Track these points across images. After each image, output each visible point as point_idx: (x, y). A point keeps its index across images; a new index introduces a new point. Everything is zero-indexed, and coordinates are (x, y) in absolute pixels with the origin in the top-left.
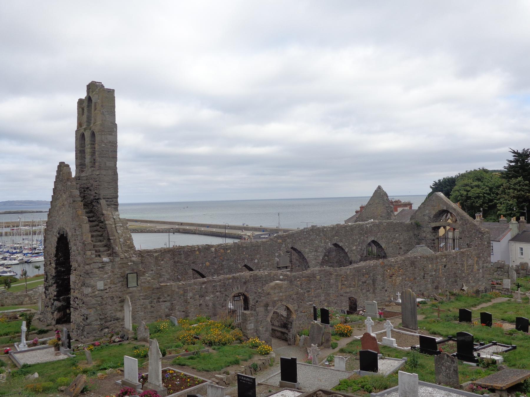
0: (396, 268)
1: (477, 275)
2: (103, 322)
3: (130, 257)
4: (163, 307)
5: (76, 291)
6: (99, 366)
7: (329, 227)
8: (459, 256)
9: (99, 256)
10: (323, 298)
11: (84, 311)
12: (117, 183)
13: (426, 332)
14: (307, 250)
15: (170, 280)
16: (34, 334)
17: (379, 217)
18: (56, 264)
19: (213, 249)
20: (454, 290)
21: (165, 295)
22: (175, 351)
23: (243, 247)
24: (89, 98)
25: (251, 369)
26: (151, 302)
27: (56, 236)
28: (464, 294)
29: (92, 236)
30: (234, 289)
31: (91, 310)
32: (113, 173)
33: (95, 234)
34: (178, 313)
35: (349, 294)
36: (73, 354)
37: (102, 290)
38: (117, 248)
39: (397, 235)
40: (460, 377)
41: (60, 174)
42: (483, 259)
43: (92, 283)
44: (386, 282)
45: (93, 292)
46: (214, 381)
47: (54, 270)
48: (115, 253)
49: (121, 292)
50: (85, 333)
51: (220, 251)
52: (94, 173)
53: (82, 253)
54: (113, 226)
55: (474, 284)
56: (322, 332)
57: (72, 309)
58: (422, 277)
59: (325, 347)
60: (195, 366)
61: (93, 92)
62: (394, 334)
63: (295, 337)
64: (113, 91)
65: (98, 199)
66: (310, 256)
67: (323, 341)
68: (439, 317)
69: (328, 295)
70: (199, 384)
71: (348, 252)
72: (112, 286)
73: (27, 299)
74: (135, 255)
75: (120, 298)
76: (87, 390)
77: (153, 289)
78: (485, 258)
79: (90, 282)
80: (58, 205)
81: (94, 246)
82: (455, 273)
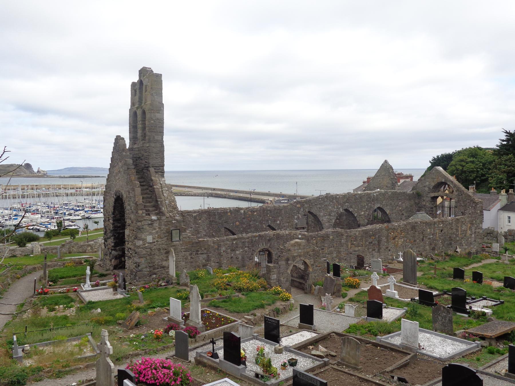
0: (399, 231)
1: (470, 239)
2: (151, 269)
3: (174, 217)
4: (201, 258)
5: (130, 243)
6: (149, 305)
7: (341, 195)
8: (454, 222)
9: (149, 215)
10: (335, 255)
11: (136, 260)
12: (163, 154)
13: (424, 287)
14: (322, 214)
15: (206, 236)
16: (96, 277)
17: (385, 187)
18: (113, 221)
19: (242, 211)
20: (449, 251)
21: (203, 249)
22: (211, 295)
23: (267, 210)
24: (141, 82)
25: (274, 312)
26: (191, 254)
27: (113, 197)
28: (457, 255)
29: (143, 198)
30: (259, 245)
31: (142, 259)
32: (160, 146)
33: (145, 196)
34: (213, 264)
35: (357, 253)
36: (128, 294)
37: (151, 243)
38: (163, 209)
39: (400, 203)
40: (454, 326)
41: (117, 145)
42: (476, 226)
43: (143, 237)
44: (389, 243)
45: (144, 245)
46: (244, 321)
47: (111, 225)
48: (162, 212)
49: (167, 245)
50: (137, 278)
51: (248, 213)
52: (145, 145)
53: (135, 212)
54: (160, 190)
55: (466, 247)
56: (334, 284)
57: (126, 258)
58: (421, 240)
59: (336, 296)
60: (227, 308)
61: (144, 76)
62: (396, 288)
63: (311, 287)
64: (161, 75)
65: (148, 167)
66: (324, 219)
67: (335, 291)
68: (435, 274)
69: (339, 252)
70: (231, 323)
71: (357, 216)
72: (159, 240)
73: (89, 248)
74: (178, 214)
75: (166, 250)
76: (140, 324)
77: (193, 244)
78: (478, 224)
79: (141, 236)
80: (115, 172)
81: (145, 206)
82: (450, 237)
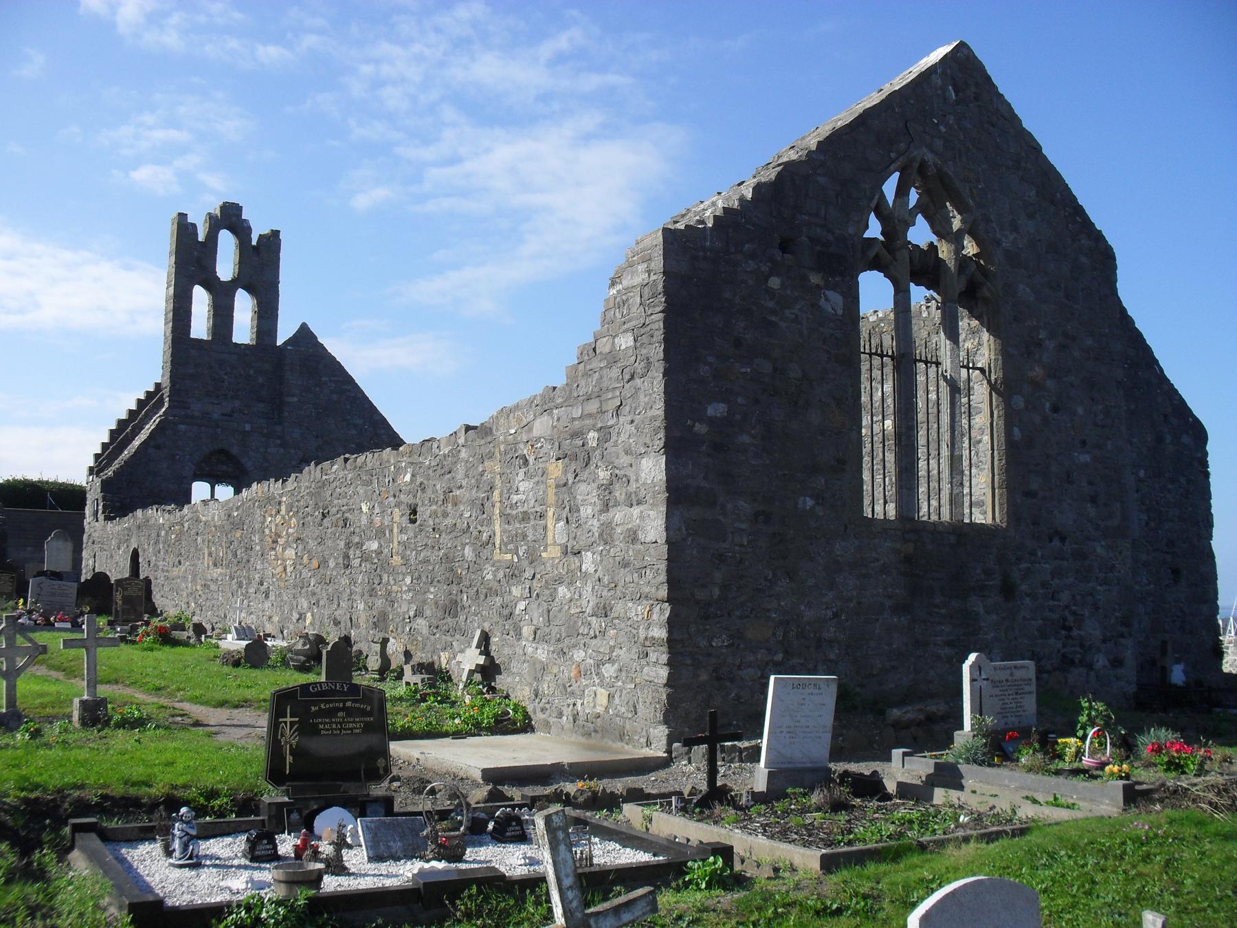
1: (562, 591)
8: (464, 454)
42: (603, 475)
58: (341, 560)
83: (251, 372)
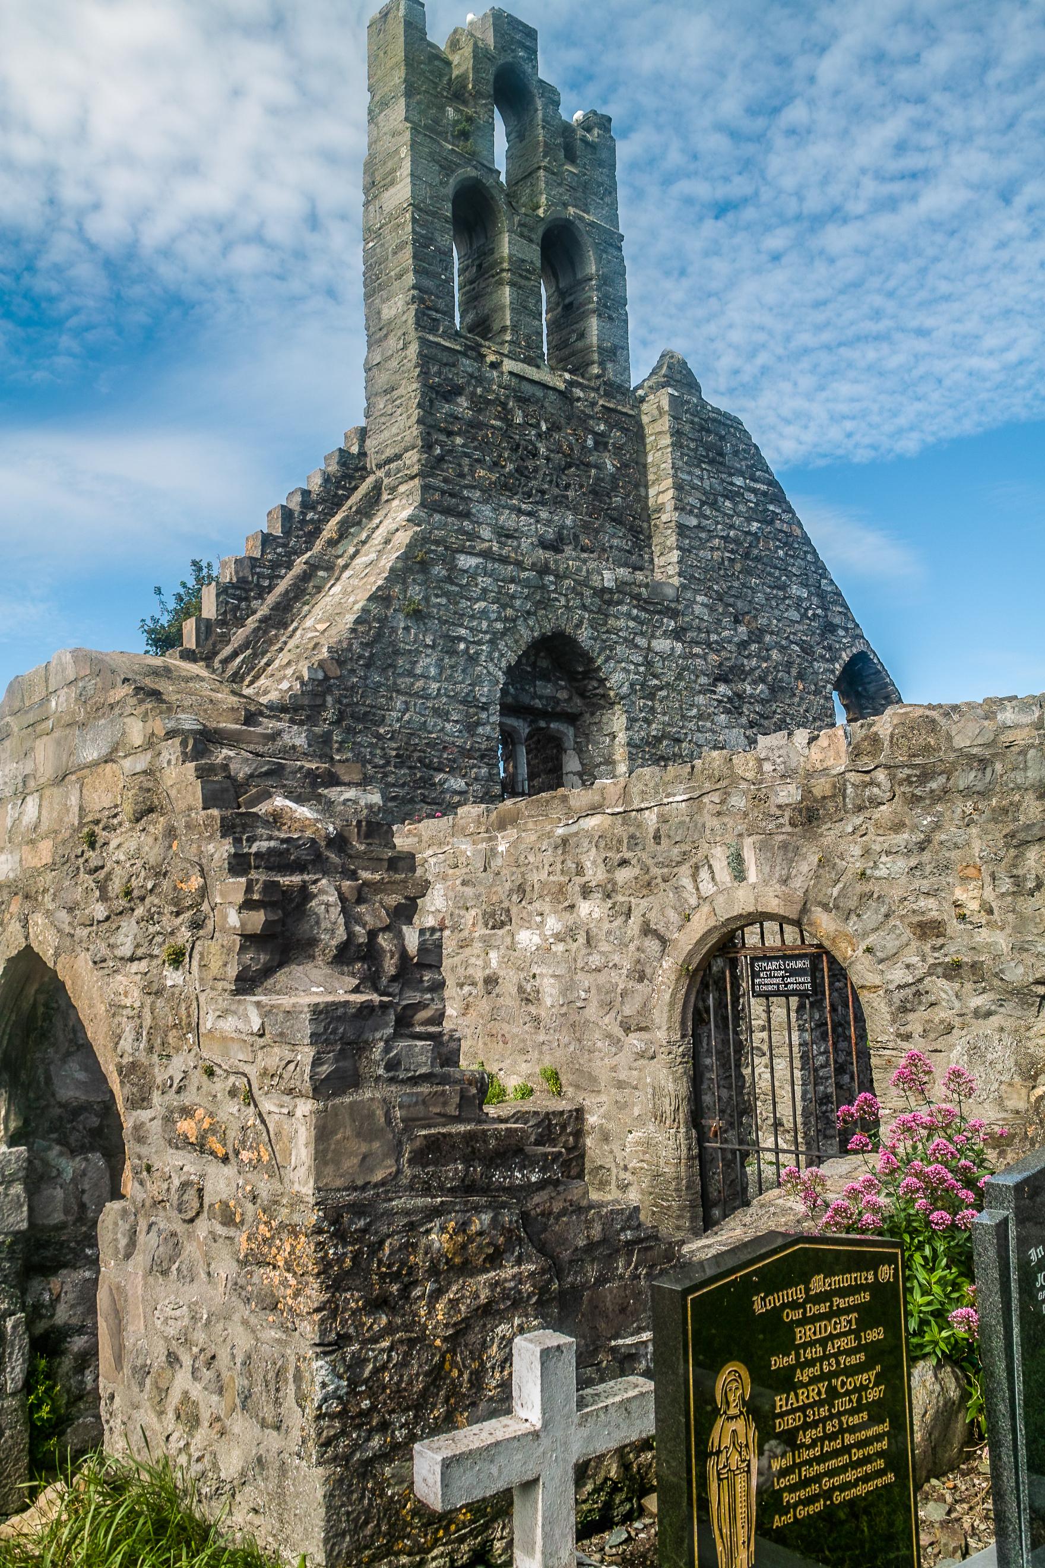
30: (704, 874)
83: (590, 443)
